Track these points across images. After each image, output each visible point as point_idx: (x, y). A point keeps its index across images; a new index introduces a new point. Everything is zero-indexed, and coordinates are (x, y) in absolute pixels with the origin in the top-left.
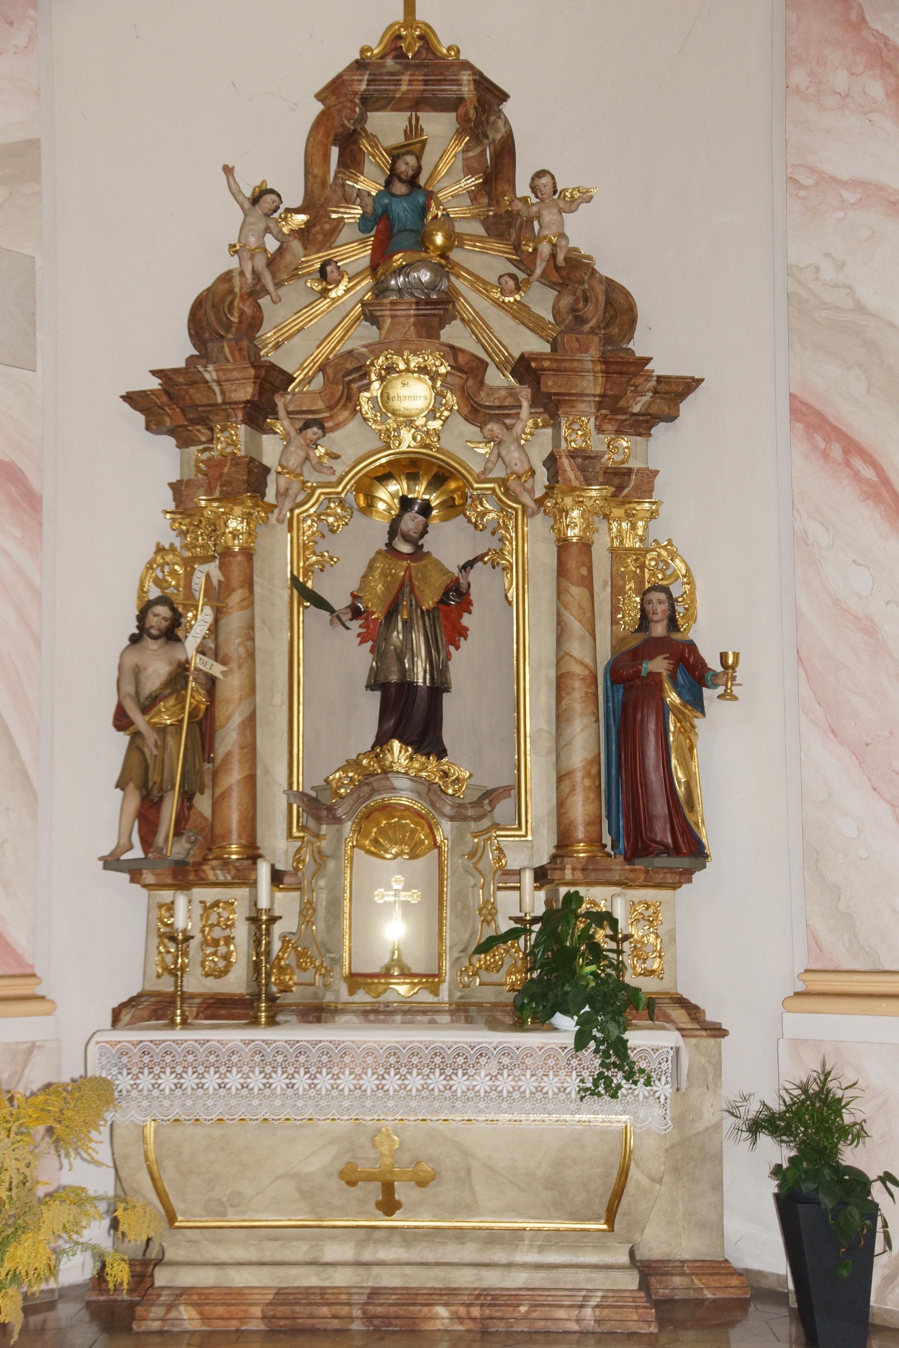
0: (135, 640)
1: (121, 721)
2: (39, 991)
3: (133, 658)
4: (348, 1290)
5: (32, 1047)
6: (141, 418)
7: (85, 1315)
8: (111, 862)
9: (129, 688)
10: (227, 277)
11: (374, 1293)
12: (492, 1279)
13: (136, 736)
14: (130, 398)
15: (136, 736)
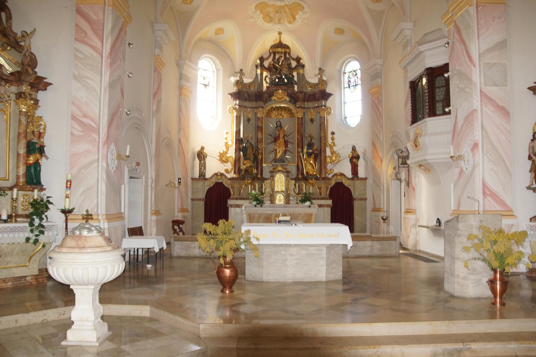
0: (532, 140)
1: (530, 158)
2: (513, 214)
3: (532, 144)
5: (512, 225)
6: (532, 92)
7: (525, 277)
8: (529, 188)
9: (531, 151)
13: (533, 161)
14: (529, 88)
15: (533, 161)
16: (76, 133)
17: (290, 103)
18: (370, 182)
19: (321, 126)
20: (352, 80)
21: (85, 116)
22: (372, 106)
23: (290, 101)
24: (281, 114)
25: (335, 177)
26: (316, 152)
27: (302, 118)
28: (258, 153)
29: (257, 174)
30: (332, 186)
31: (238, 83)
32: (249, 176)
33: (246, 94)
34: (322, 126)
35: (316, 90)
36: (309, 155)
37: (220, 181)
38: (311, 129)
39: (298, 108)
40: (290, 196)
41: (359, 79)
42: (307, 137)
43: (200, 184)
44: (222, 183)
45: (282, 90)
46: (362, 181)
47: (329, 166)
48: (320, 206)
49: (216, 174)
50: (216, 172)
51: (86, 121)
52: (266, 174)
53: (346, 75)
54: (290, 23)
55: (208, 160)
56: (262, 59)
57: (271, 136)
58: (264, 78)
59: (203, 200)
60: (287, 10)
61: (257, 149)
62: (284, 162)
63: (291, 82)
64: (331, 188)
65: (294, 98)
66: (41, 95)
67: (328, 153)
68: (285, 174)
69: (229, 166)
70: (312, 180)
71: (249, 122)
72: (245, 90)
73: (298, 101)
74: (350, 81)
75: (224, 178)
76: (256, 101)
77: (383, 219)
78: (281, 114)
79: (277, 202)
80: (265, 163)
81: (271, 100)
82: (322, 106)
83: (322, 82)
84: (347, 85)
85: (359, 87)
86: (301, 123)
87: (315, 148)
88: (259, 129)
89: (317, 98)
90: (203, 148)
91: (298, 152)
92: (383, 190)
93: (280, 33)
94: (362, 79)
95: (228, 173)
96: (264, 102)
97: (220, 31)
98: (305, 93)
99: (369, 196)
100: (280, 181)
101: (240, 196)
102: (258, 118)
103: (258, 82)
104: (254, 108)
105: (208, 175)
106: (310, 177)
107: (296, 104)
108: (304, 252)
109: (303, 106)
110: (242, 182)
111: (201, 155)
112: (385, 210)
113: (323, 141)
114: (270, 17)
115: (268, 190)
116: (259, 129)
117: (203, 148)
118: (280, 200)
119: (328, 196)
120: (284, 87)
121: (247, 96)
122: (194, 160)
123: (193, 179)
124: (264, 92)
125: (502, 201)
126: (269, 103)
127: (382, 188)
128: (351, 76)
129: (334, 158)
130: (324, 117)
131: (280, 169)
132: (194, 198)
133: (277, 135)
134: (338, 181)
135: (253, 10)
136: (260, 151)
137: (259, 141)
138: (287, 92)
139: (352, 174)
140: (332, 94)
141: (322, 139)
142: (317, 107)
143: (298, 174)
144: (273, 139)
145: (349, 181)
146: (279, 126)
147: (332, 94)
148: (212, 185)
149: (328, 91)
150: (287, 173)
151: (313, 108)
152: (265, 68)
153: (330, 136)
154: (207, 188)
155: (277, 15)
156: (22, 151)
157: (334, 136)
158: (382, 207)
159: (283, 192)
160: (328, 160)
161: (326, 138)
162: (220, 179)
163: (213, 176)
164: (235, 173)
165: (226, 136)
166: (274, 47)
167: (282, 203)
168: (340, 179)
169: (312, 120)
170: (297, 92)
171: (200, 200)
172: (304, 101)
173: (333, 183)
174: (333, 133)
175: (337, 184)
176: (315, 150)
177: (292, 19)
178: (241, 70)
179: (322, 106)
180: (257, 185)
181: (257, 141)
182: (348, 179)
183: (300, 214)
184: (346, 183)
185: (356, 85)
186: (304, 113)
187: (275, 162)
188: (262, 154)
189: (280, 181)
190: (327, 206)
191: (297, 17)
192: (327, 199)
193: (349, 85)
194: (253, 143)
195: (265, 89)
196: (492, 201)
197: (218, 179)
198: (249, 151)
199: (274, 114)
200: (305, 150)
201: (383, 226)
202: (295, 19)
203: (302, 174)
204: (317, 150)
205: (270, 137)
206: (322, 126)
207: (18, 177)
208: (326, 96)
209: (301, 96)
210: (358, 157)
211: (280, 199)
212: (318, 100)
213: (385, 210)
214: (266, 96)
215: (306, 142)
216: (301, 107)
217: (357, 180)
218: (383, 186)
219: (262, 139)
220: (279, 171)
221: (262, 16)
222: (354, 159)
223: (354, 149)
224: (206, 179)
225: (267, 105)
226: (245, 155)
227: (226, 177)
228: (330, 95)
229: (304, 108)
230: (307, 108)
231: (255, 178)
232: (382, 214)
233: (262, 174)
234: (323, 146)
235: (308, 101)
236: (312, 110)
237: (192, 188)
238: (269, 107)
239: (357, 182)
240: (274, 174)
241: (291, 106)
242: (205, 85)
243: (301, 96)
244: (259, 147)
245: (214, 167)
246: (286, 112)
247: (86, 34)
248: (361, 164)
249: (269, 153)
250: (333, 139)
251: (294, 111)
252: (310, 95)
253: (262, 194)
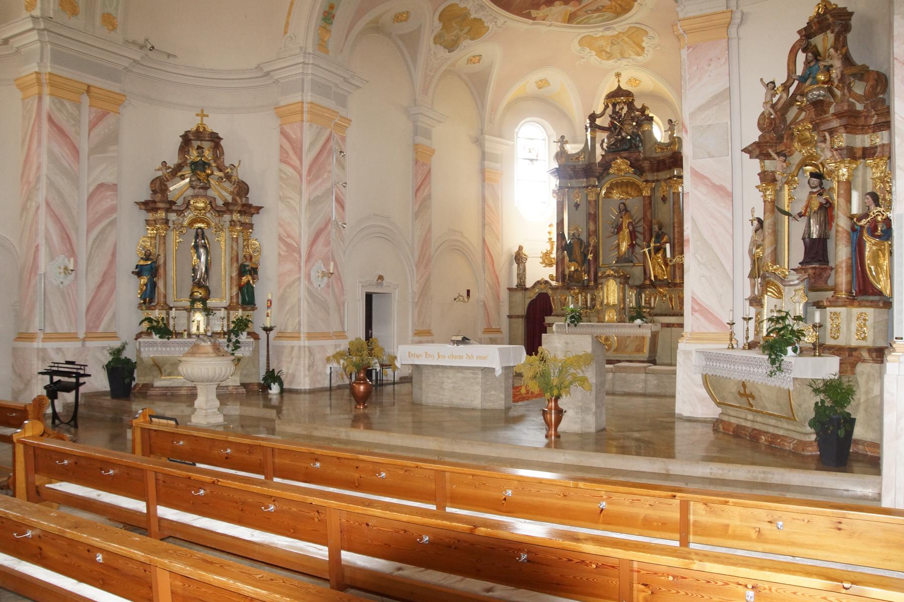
4: (748, 428)
10: (763, 114)
11: (754, 429)
12: (776, 431)
16: (283, 253)
21: (289, 236)
23: (635, 173)
27: (650, 197)
29: (589, 280)
34: (676, 206)
37: (544, 291)
38: (664, 213)
43: (519, 295)
44: (546, 294)
45: (622, 158)
51: (289, 240)
54: (639, 55)
55: (529, 265)
56: (593, 117)
59: (522, 317)
60: (626, 39)
65: (638, 168)
66: (255, 219)
69: (552, 271)
70: (661, 287)
81: (608, 174)
83: (675, 141)
86: (649, 203)
90: (521, 248)
93: (618, 75)
97: (542, 84)
102: (590, 202)
103: (589, 151)
105: (529, 284)
108: (460, 375)
110: (567, 292)
111: (519, 258)
114: (606, 52)
116: (593, 217)
117: (521, 248)
121: (577, 172)
122: (511, 265)
123: (510, 289)
125: (717, 318)
132: (513, 313)
135: (579, 48)
143: (645, 279)
148: (534, 297)
151: (665, 180)
154: (528, 301)
155: (615, 47)
156: (235, 274)
163: (535, 284)
165: (549, 229)
166: (611, 96)
171: (518, 317)
177: (638, 49)
179: (674, 176)
183: (629, 337)
191: (644, 44)
195: (599, 159)
196: (701, 318)
198: (577, 251)
200: (652, 245)
202: (643, 49)
207: (231, 298)
212: (670, 168)
214: (599, 170)
220: (609, 276)
221: (594, 53)
224: (526, 289)
226: (570, 255)
231: (584, 288)
235: (658, 171)
237: (510, 302)
241: (636, 179)
242: (532, 160)
245: (539, 272)
247: (287, 153)
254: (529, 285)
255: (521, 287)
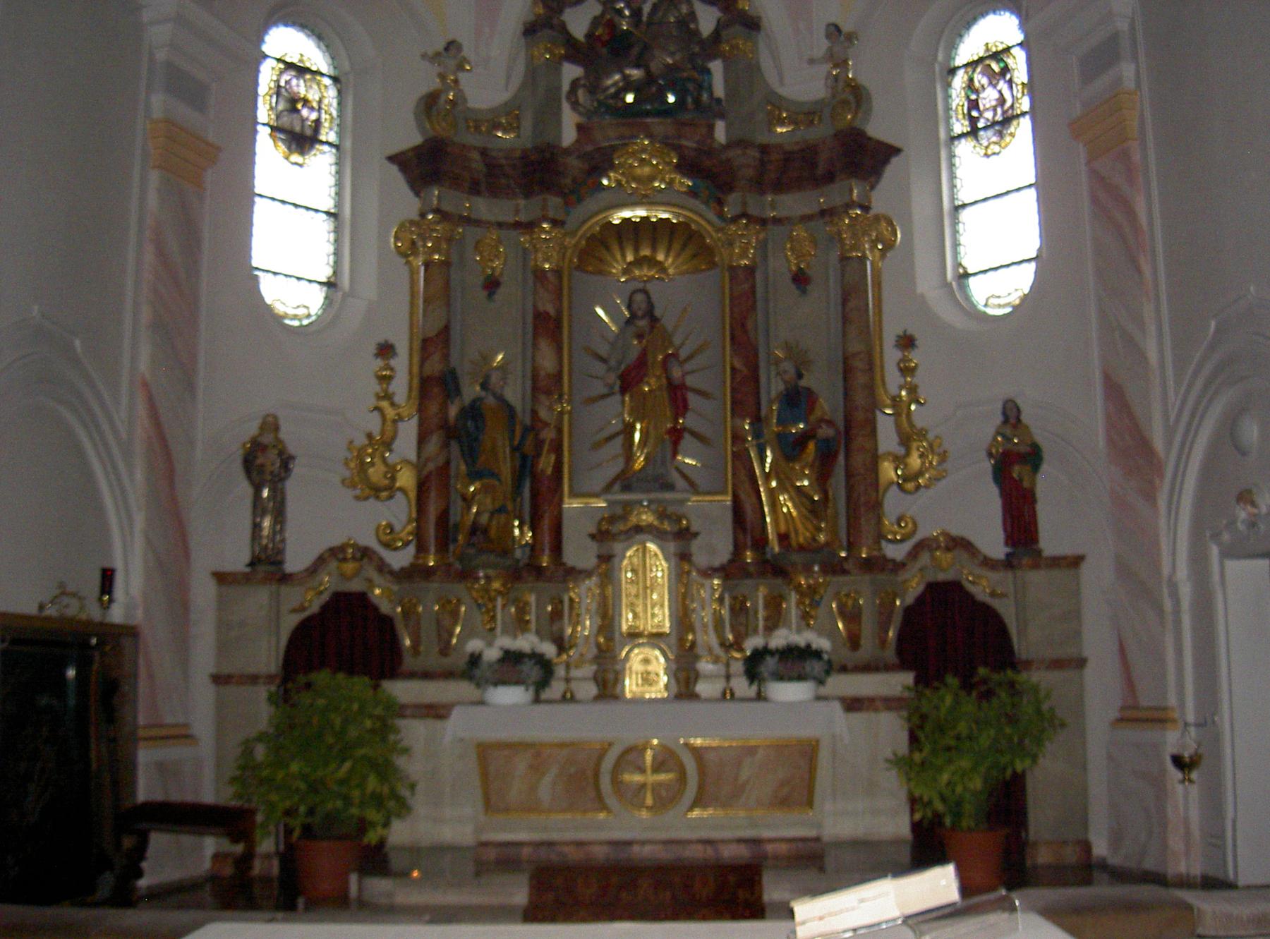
17: (692, 202)
18: (1097, 578)
19: (845, 302)
20: (989, 97)
22: (1095, 200)
24: (651, 262)
25: (925, 558)
26: (825, 431)
27: (750, 270)
28: (539, 444)
29: (534, 548)
30: (910, 600)
31: (429, 103)
32: (492, 557)
33: (476, 156)
35: (820, 132)
36: (791, 449)
37: (355, 586)
38: (798, 325)
39: (735, 220)
40: (697, 658)
41: (1018, 91)
42: (778, 361)
43: (259, 598)
45: (650, 136)
46: (1056, 573)
47: (893, 503)
48: (853, 704)
49: (336, 553)
50: (336, 542)
52: (578, 552)
53: (959, 80)
55: (299, 490)
57: (604, 360)
58: (566, 87)
59: (270, 678)
61: (536, 425)
62: (670, 487)
63: (697, 102)
64: (908, 611)
65: (709, 174)
67: (887, 438)
68: (672, 546)
69: (398, 512)
70: (807, 570)
71: (490, 295)
72: (471, 139)
73: (728, 187)
74: (974, 105)
75: (372, 573)
76: (528, 194)
77: (1178, 761)
78: (651, 262)
79: (631, 686)
80: (574, 494)
82: (850, 205)
84: (960, 126)
85: (1024, 129)
87: (818, 413)
88: (547, 326)
89: (820, 170)
91: (738, 438)
92: (1177, 611)
94: (1030, 87)
95: (387, 545)
96: (561, 193)
98: (764, 149)
99: (1097, 643)
100: (648, 586)
101: (447, 662)
102: (540, 275)
104: (517, 225)
106: (796, 558)
107: (720, 203)
109: (753, 211)
110: (459, 589)
112: (1191, 718)
113: (861, 379)
115: (587, 626)
116: (547, 326)
117: (271, 425)
118: (647, 679)
119: (890, 654)
120: (659, 126)
123: (222, 578)
124: (567, 152)
126: (590, 204)
127: (1168, 605)
128: (980, 79)
129: (915, 461)
130: (864, 257)
131: (647, 518)
133: (633, 355)
134: (941, 577)
136: (548, 435)
137: (545, 386)
138: (678, 149)
139: (1006, 544)
140: (896, 151)
141: (857, 370)
142: (823, 213)
143: (738, 550)
144: (612, 378)
145: (995, 576)
146: (644, 316)
147: (896, 151)
148: (315, 608)
149: (878, 129)
150: (680, 538)
151: (806, 219)
152: (570, 41)
153: (891, 356)
154: (291, 622)
157: (915, 357)
158: (1172, 700)
159: (659, 635)
160: (888, 471)
161: (872, 365)
162: (357, 573)
163: (321, 561)
164: (421, 549)
167: (660, 687)
168: (948, 567)
169: (800, 280)
170: (729, 146)
171: (254, 679)
172: (759, 185)
173: (914, 587)
174: (907, 342)
175: (932, 588)
176: (822, 420)
178: (451, 46)
180: (532, 599)
181: (535, 389)
182: (988, 563)
183: (751, 751)
184: (981, 586)
185: (1007, 120)
186: (763, 246)
187: (627, 488)
188: (557, 448)
189: (648, 586)
190: (890, 703)
192: (888, 668)
193: (974, 121)
194: (514, 393)
197: (343, 576)
199: (620, 263)
201: (1185, 798)
203: (760, 543)
204: (830, 423)
205: (600, 368)
206: (854, 303)
208: (865, 157)
209: (745, 161)
210: (1033, 457)
211: (646, 673)
212: (830, 178)
213: (1191, 718)
214: (574, 164)
215: (772, 387)
216: (744, 215)
217: (1036, 566)
218: (1175, 595)
219: (559, 376)
220: (638, 529)
222: (1015, 466)
223: (1011, 416)
224: (285, 578)
225: (579, 212)
227: (382, 567)
228: (888, 152)
229: (763, 222)
230: (777, 221)
232: (1172, 741)
233: (557, 549)
234: (860, 398)
235: (780, 187)
236: (799, 232)
237: (223, 626)
238: (594, 225)
239: (1036, 578)
240: (617, 547)
243: (745, 161)
244: (543, 414)
245: (329, 519)
246: (676, 246)
248: (1049, 487)
249: (597, 446)
250: (906, 370)
251: (712, 237)
252: (788, 157)
253: (562, 645)
254: (295, 561)
255: (267, 564)
